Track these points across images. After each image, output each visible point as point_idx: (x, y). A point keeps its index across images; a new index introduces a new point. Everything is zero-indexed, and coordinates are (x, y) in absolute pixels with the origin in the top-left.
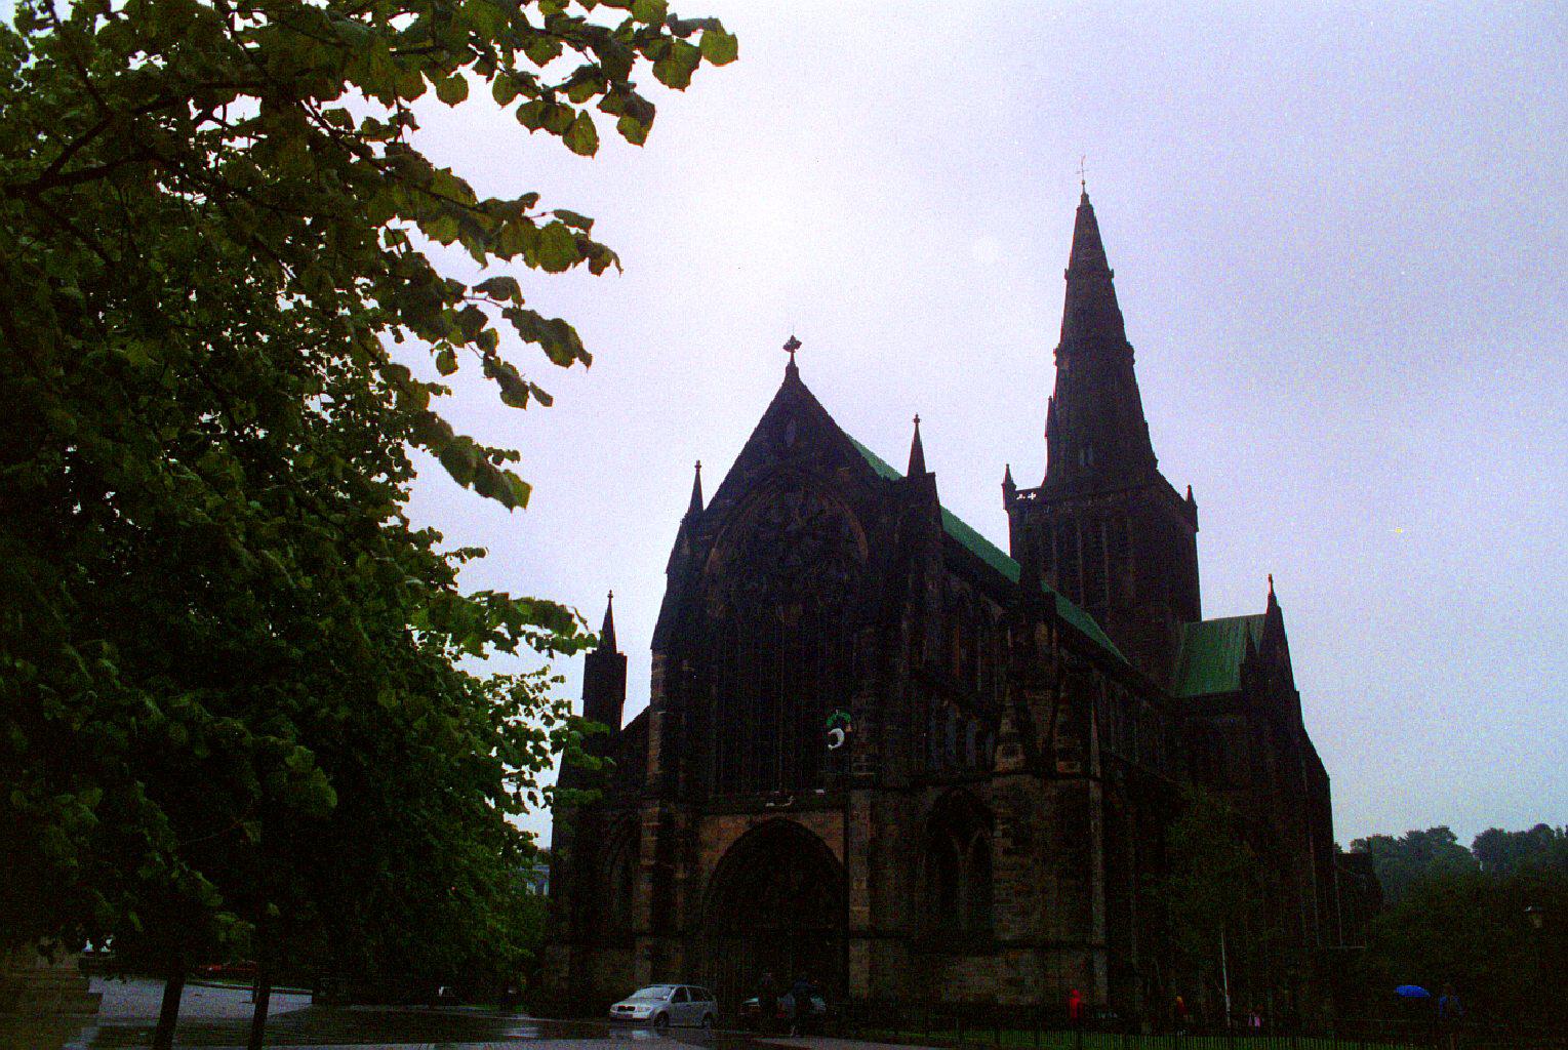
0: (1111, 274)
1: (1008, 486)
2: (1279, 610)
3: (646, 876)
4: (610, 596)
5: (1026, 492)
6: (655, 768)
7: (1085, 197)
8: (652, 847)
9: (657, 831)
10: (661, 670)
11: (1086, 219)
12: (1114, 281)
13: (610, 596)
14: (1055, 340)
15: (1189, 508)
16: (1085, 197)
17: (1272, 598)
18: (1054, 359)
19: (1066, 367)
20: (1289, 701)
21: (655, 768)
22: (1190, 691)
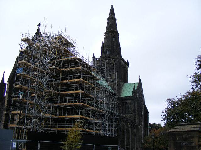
0: (116, 20)
1: (94, 57)
2: (141, 82)
3: (2, 125)
4: (4, 72)
5: (97, 58)
6: (6, 104)
7: (112, 6)
8: (4, 119)
9: (6, 117)
10: (9, 86)
11: (112, 9)
12: (116, 21)
13: (4, 72)
14: (105, 31)
15: (127, 63)
16: (112, 6)
17: (140, 79)
18: (104, 34)
19: (106, 36)
20: (142, 98)
21: (6, 104)
22: (121, 96)
